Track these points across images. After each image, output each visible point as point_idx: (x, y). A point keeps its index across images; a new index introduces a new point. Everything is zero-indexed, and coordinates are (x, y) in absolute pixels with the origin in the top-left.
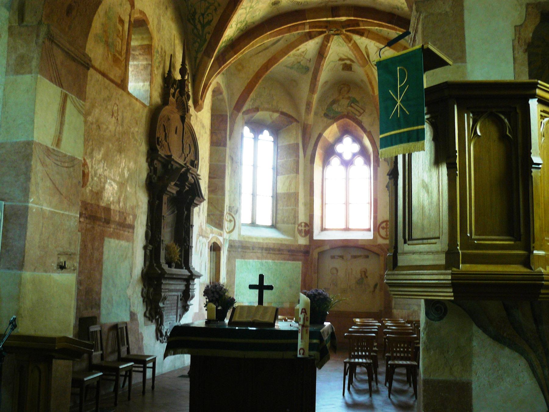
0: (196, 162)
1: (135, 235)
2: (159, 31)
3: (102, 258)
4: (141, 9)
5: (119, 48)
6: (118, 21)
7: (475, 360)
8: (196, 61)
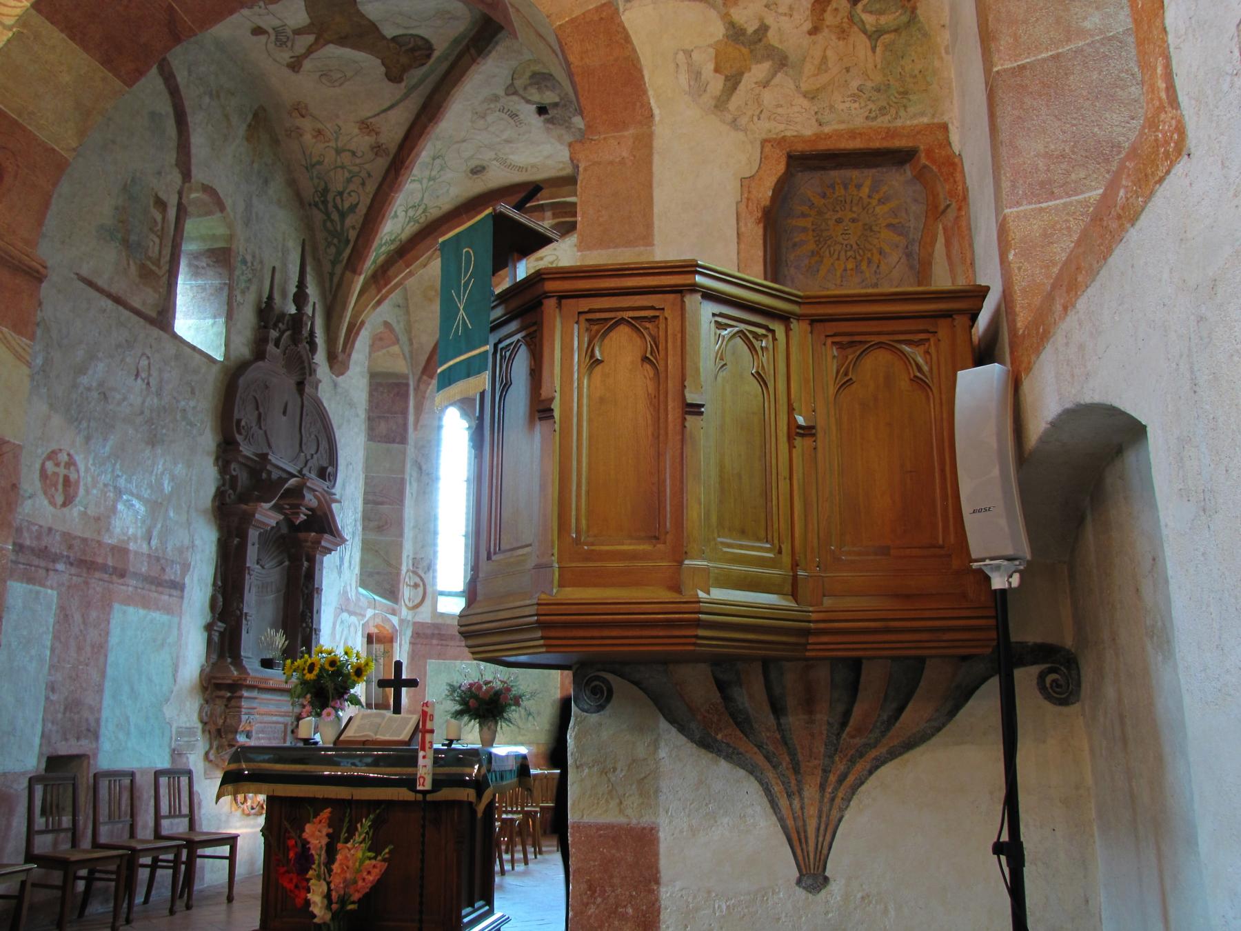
0: (330, 469)
1: (186, 601)
2: (247, 223)
3: (107, 641)
4: (206, 182)
5: (154, 251)
6: (152, 203)
7: (664, 784)
8: (331, 280)
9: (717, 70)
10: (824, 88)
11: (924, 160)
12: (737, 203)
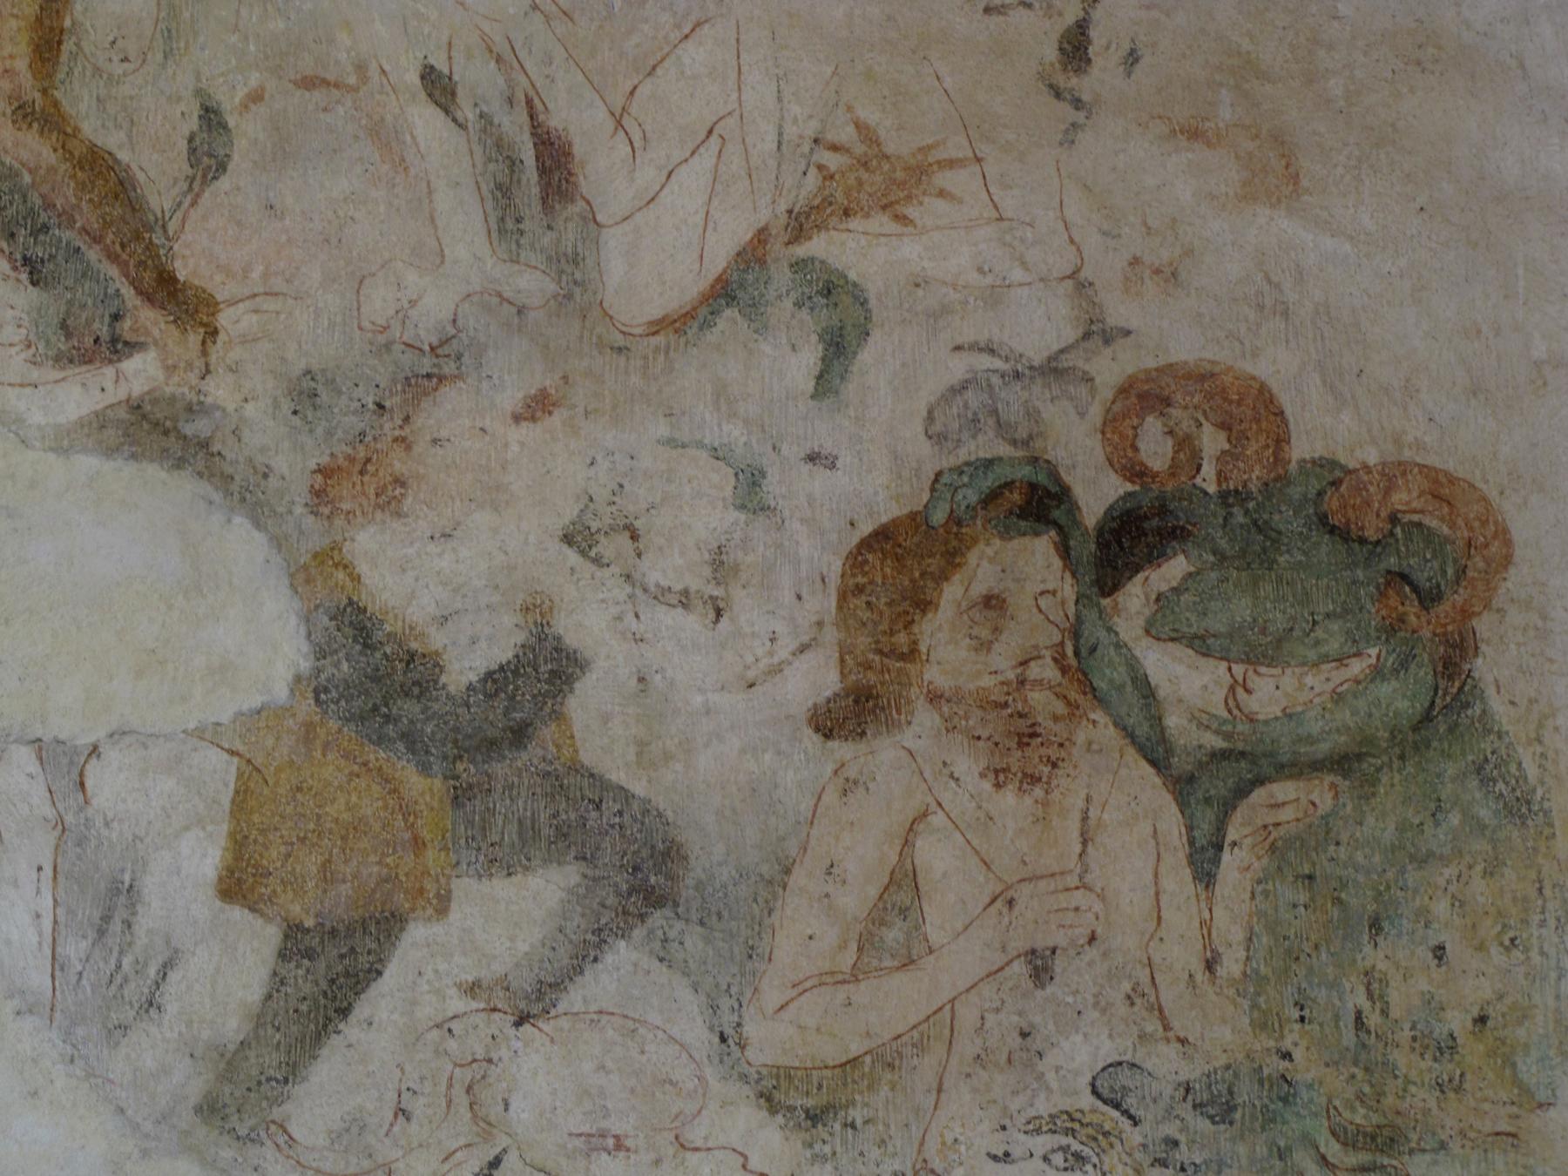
9: (237, 885)
10: (886, 1060)
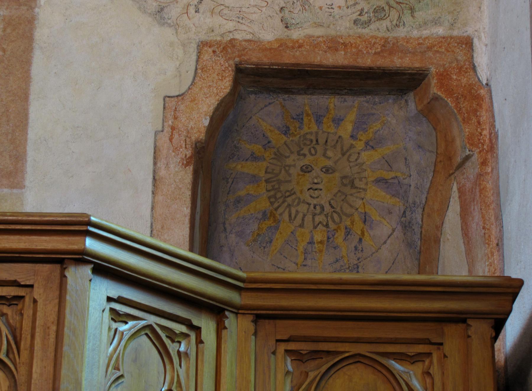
11: (434, 90)
12: (156, 133)
